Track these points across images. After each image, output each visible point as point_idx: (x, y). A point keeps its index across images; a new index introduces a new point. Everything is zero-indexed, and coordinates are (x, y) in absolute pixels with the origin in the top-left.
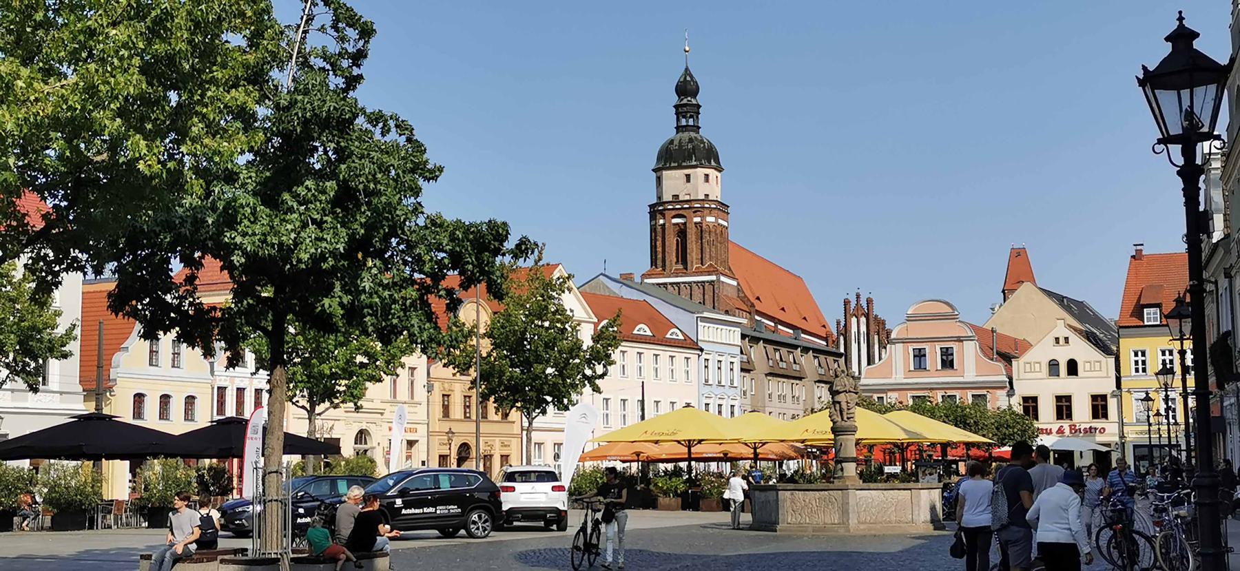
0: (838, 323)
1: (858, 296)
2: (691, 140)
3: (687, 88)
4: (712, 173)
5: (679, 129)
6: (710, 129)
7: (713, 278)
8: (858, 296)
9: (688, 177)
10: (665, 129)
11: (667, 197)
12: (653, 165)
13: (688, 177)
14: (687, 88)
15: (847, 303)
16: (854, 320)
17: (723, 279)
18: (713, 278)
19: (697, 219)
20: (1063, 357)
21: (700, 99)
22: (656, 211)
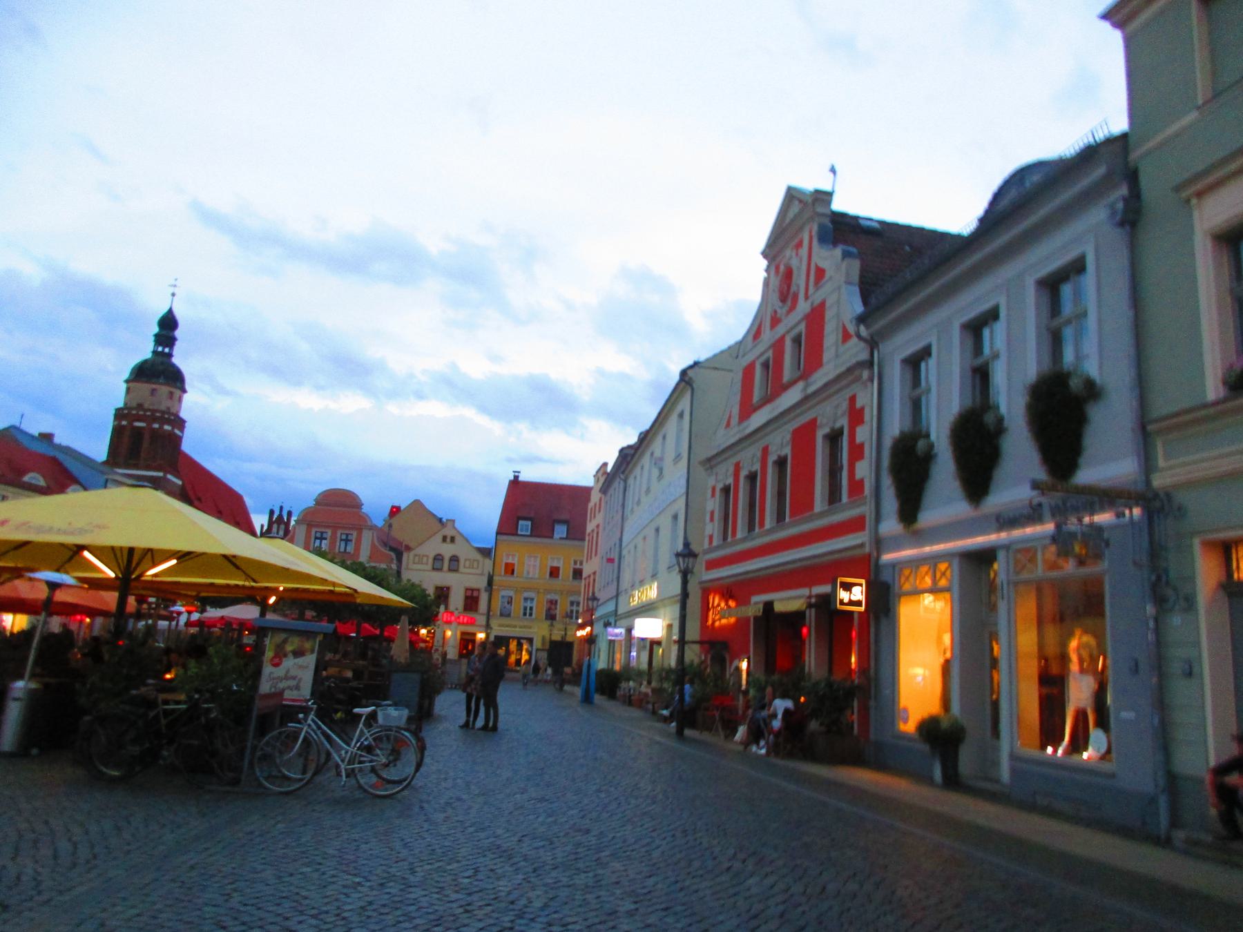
0: (262, 526)
1: (281, 508)
2: (162, 363)
3: (168, 324)
4: (177, 392)
5: (155, 352)
6: (180, 359)
7: (161, 474)
8: (281, 508)
9: (153, 391)
10: (145, 350)
11: (134, 405)
12: (126, 375)
13: (153, 391)
14: (168, 324)
15: (272, 512)
16: (275, 526)
17: (169, 476)
18: (161, 474)
19: (156, 426)
20: (447, 550)
21: (178, 333)
22: (119, 414)
